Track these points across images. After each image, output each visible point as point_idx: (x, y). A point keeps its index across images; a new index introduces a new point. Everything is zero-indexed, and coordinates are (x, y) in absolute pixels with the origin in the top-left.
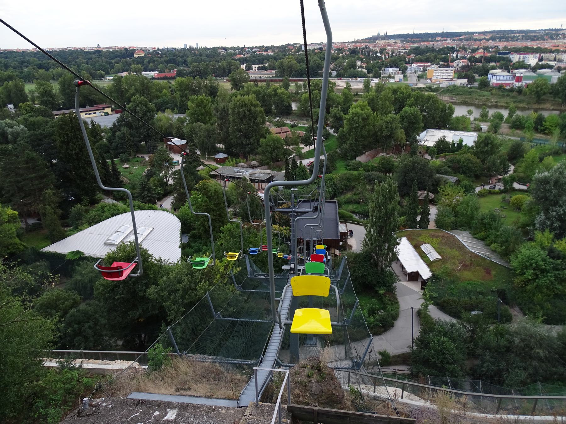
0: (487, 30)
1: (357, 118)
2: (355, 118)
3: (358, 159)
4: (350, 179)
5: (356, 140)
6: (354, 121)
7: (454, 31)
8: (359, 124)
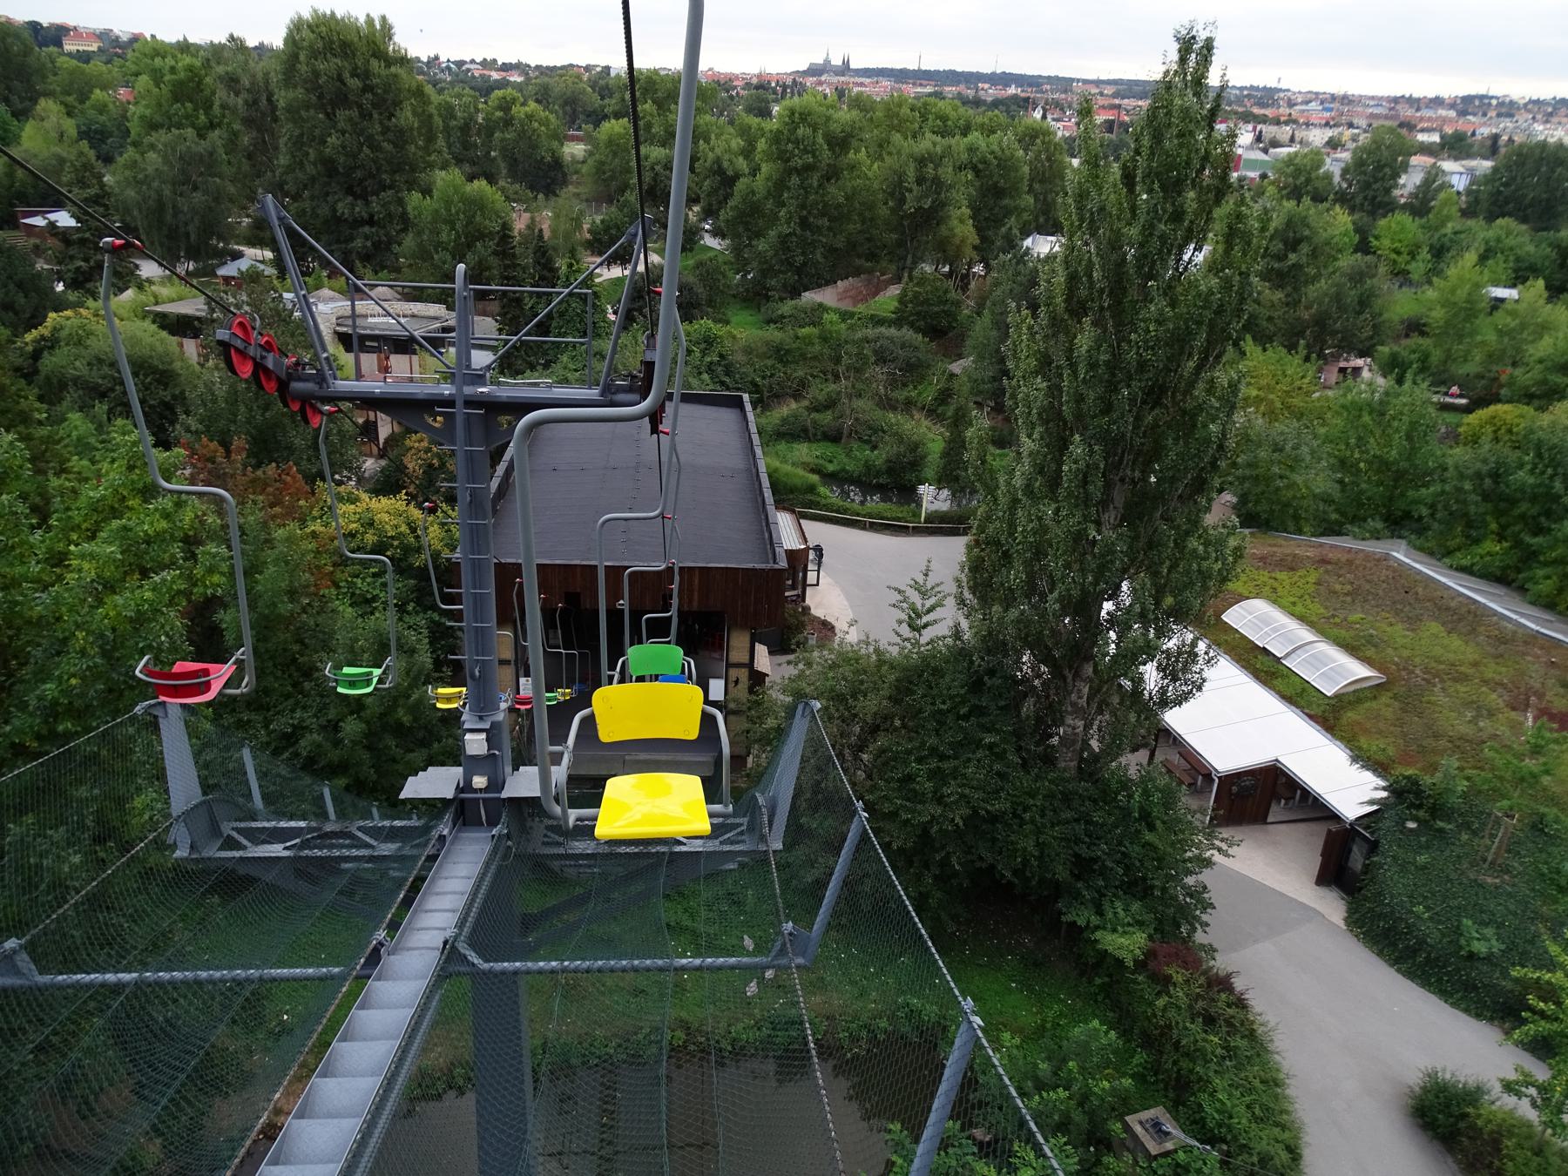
0: (1104, 77)
1: (809, 131)
2: (800, 132)
3: (810, 297)
4: (788, 352)
5: (804, 223)
6: (797, 142)
7: (1022, 72)
8: (814, 156)
